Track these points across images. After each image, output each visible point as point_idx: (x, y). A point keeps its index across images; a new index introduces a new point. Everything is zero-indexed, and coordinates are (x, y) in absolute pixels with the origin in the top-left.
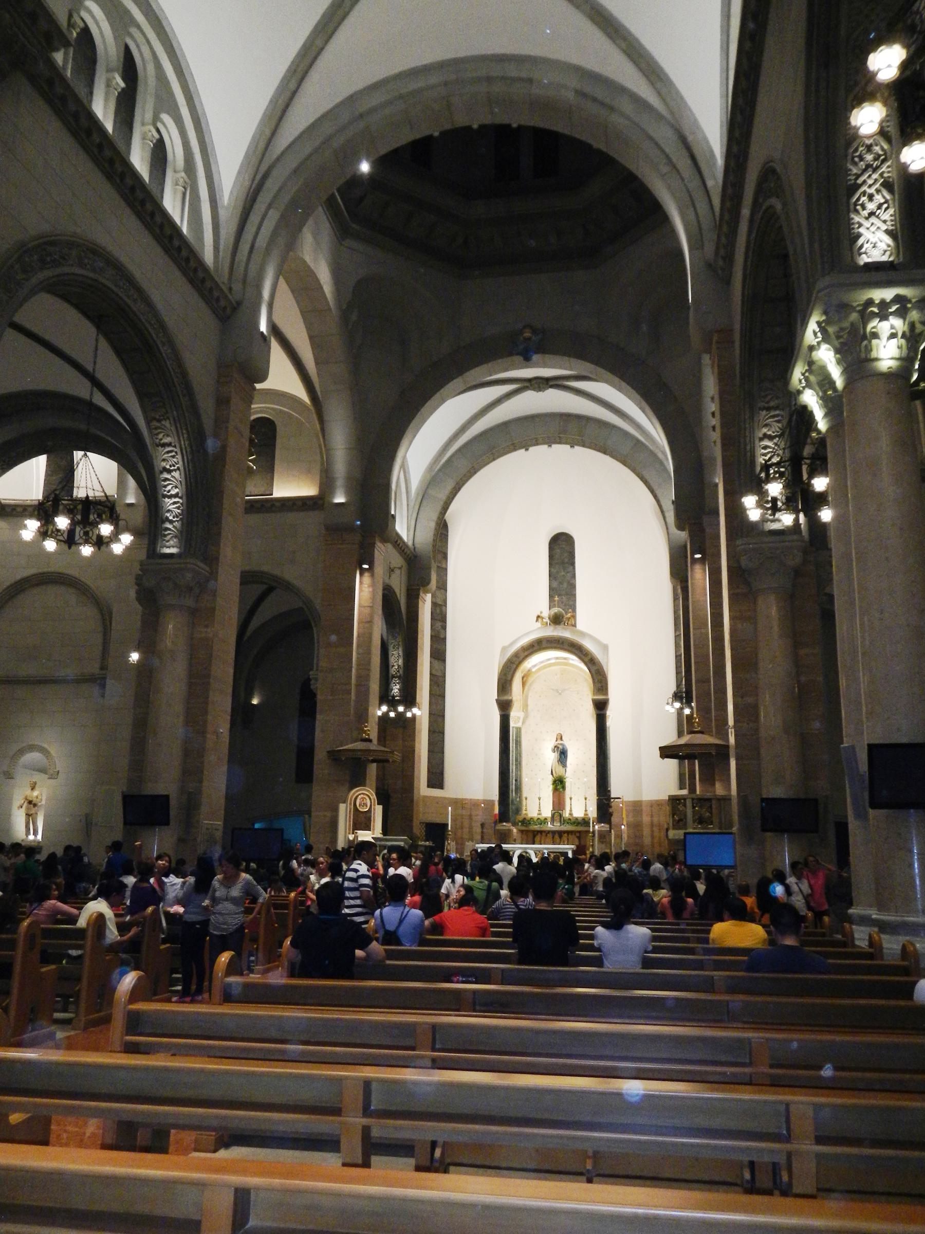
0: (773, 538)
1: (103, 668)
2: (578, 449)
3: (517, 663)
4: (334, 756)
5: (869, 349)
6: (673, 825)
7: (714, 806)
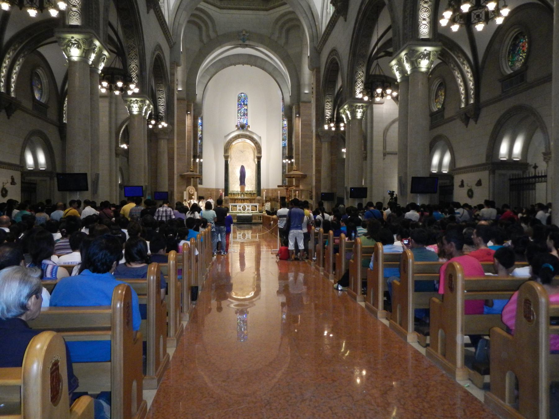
2: (253, 67)
4: (182, 177)
5: (356, 114)
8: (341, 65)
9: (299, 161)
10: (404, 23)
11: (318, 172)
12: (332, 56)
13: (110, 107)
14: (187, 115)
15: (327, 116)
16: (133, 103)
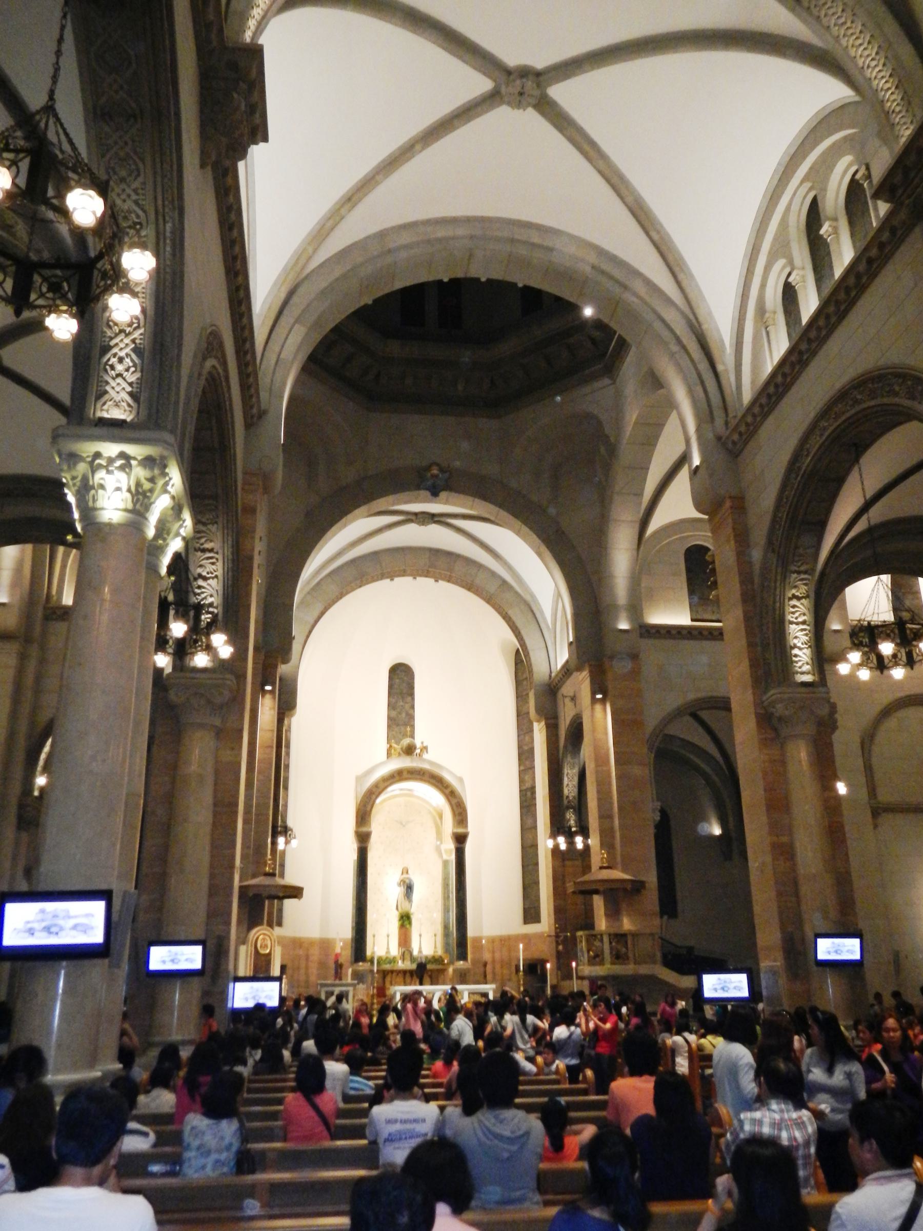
0: (803, 690)
2: (442, 583)
3: (377, 793)
6: (589, 961)
7: (629, 942)
9: (613, 837)
13: (20, 671)
14: (263, 696)
15: (795, 646)
16: (106, 467)
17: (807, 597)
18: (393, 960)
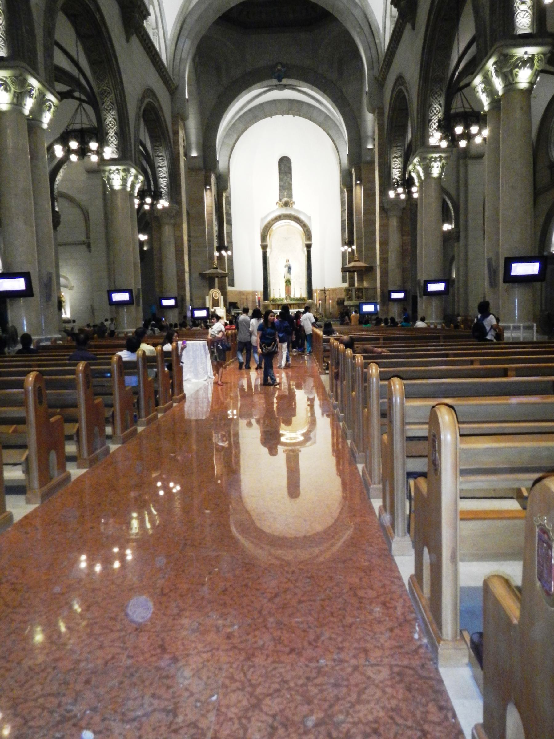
1: (88, 237)
2: (297, 117)
5: (431, 171)
8: (409, 100)
10: (492, 12)
11: (384, 260)
12: (398, 86)
17: (401, 157)
18: (283, 300)
